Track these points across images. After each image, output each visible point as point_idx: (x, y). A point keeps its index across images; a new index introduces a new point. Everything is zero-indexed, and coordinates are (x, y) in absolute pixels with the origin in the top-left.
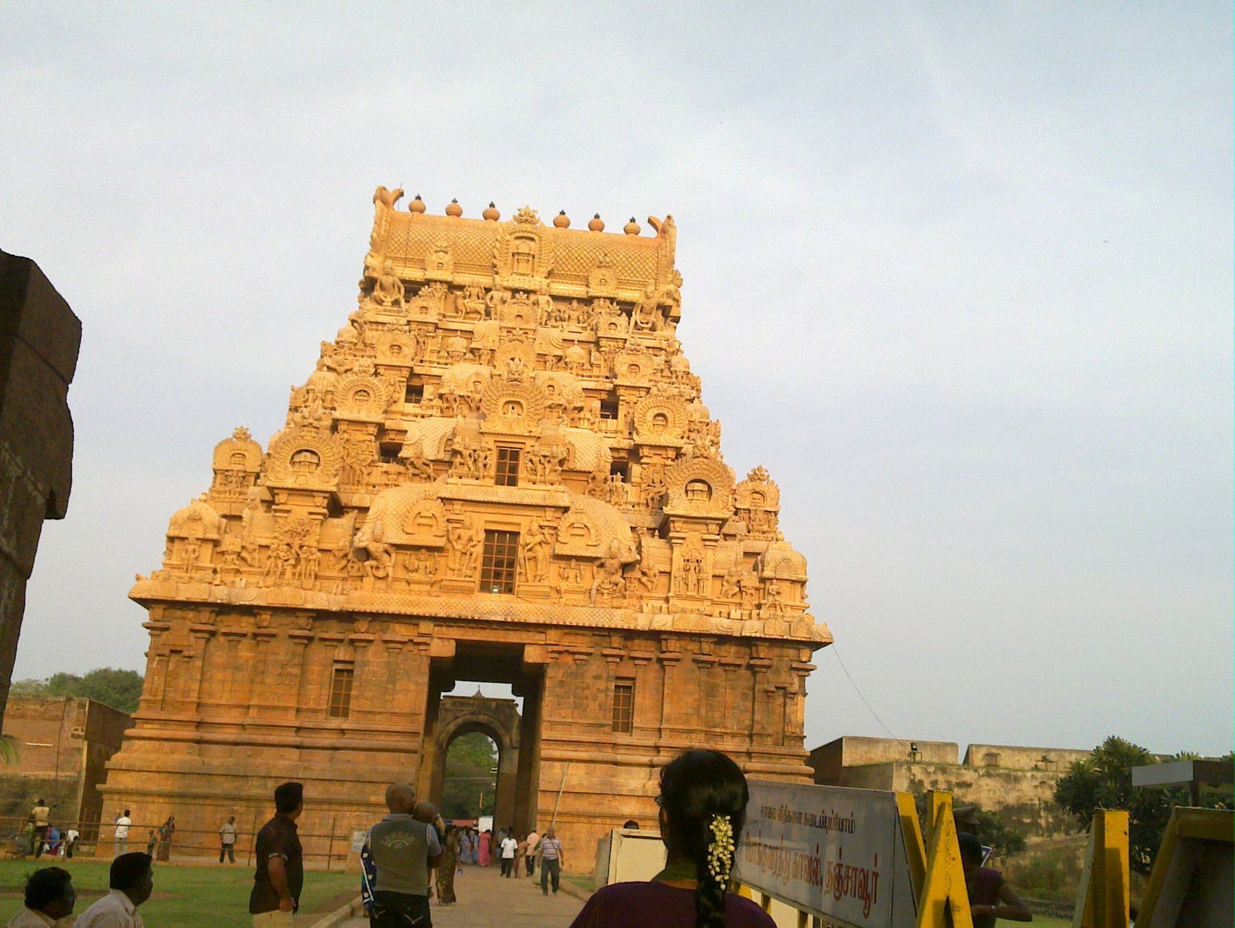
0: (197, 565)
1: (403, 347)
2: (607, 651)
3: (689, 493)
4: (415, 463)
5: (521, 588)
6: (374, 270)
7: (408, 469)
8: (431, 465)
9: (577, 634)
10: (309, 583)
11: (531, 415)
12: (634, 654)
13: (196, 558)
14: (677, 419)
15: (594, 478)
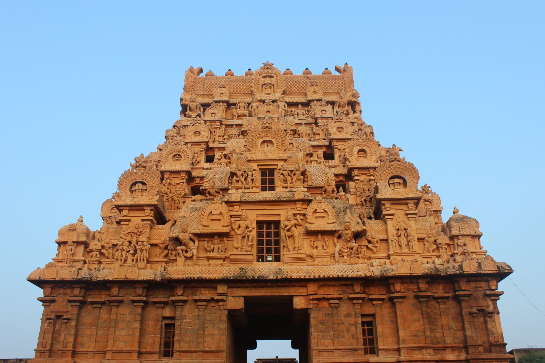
0: (73, 258)
1: (201, 132)
2: (352, 296)
3: (391, 186)
4: (211, 191)
5: (286, 256)
6: (186, 101)
7: (207, 196)
8: (221, 192)
9: (329, 286)
10: (142, 264)
11: (279, 147)
12: (371, 297)
13: (73, 254)
14: (372, 151)
15: (325, 191)
